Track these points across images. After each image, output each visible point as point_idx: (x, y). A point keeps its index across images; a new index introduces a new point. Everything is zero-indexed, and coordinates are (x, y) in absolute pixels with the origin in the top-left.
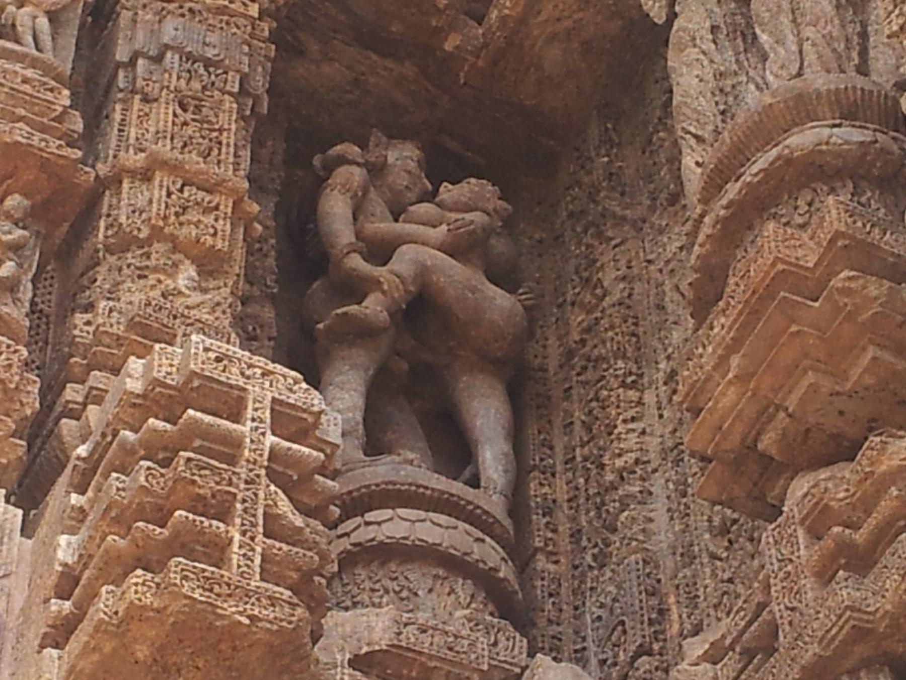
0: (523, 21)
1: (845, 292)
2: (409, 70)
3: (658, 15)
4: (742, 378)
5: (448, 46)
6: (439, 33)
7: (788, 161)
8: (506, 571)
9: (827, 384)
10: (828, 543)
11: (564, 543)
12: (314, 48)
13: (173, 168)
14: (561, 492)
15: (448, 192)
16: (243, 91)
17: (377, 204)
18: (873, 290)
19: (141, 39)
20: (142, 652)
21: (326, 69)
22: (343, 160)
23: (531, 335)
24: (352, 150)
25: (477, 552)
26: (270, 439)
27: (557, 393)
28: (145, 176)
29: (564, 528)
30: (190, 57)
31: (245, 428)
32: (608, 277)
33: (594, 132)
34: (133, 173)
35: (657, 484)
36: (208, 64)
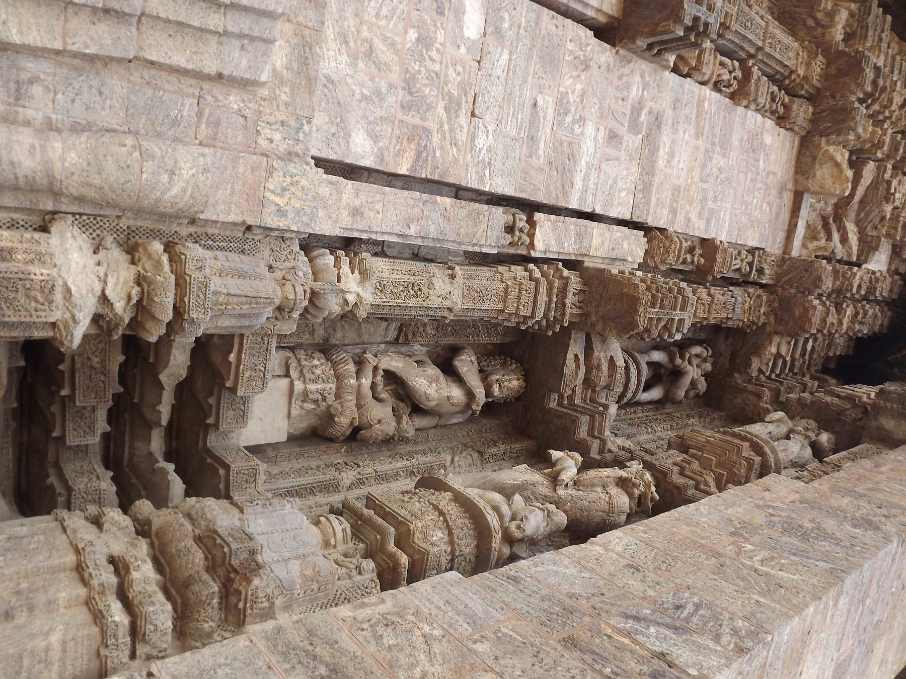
0: (747, 391)
1: (740, 463)
2: (727, 366)
3: (767, 419)
4: (708, 442)
5: (736, 375)
6: (739, 372)
7: (762, 448)
8: (625, 400)
9: (714, 463)
10: (684, 464)
11: (629, 417)
12: (729, 342)
13: (712, 301)
14: (640, 415)
15: (703, 379)
16: (728, 318)
17: (699, 360)
18: (742, 471)
19: (735, 292)
20: (625, 290)
21: (723, 346)
22: (707, 350)
23: (673, 403)
24: (710, 353)
25: (630, 391)
26: (677, 318)
27: (661, 412)
28: (709, 295)
29: (632, 416)
30: (734, 305)
31: (678, 312)
32: (692, 420)
33: (721, 414)
34: (709, 291)
35: (651, 436)
36: (734, 309)
